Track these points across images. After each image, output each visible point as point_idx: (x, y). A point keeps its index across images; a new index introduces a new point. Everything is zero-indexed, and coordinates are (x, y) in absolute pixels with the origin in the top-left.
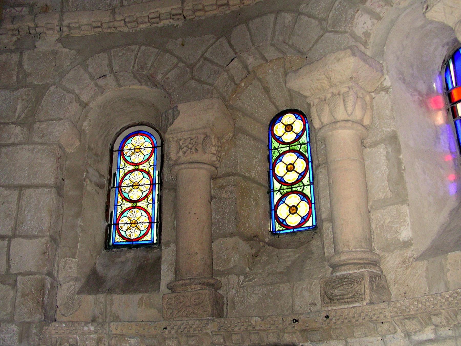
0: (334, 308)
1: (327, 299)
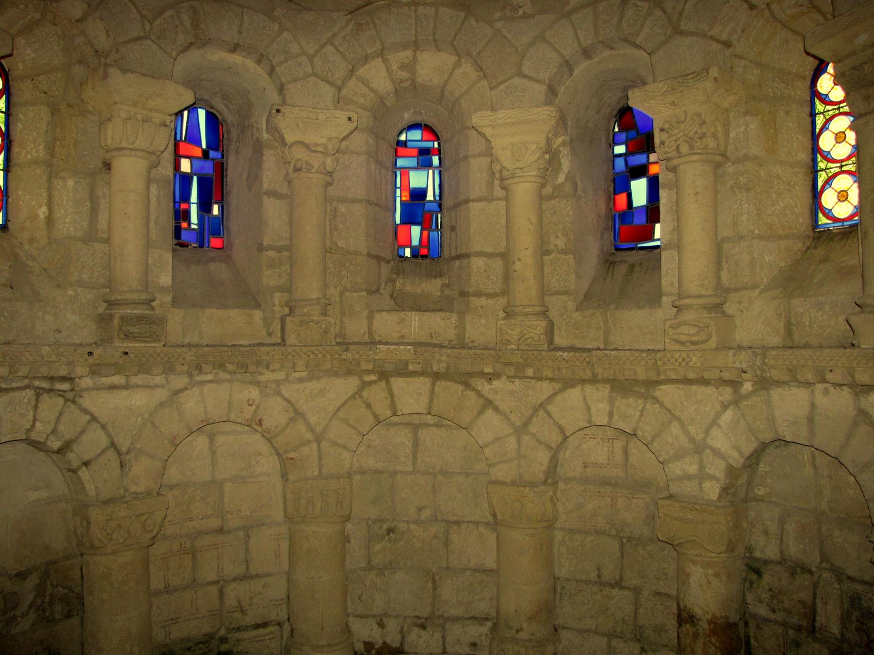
0: (130, 345)
1: (122, 336)
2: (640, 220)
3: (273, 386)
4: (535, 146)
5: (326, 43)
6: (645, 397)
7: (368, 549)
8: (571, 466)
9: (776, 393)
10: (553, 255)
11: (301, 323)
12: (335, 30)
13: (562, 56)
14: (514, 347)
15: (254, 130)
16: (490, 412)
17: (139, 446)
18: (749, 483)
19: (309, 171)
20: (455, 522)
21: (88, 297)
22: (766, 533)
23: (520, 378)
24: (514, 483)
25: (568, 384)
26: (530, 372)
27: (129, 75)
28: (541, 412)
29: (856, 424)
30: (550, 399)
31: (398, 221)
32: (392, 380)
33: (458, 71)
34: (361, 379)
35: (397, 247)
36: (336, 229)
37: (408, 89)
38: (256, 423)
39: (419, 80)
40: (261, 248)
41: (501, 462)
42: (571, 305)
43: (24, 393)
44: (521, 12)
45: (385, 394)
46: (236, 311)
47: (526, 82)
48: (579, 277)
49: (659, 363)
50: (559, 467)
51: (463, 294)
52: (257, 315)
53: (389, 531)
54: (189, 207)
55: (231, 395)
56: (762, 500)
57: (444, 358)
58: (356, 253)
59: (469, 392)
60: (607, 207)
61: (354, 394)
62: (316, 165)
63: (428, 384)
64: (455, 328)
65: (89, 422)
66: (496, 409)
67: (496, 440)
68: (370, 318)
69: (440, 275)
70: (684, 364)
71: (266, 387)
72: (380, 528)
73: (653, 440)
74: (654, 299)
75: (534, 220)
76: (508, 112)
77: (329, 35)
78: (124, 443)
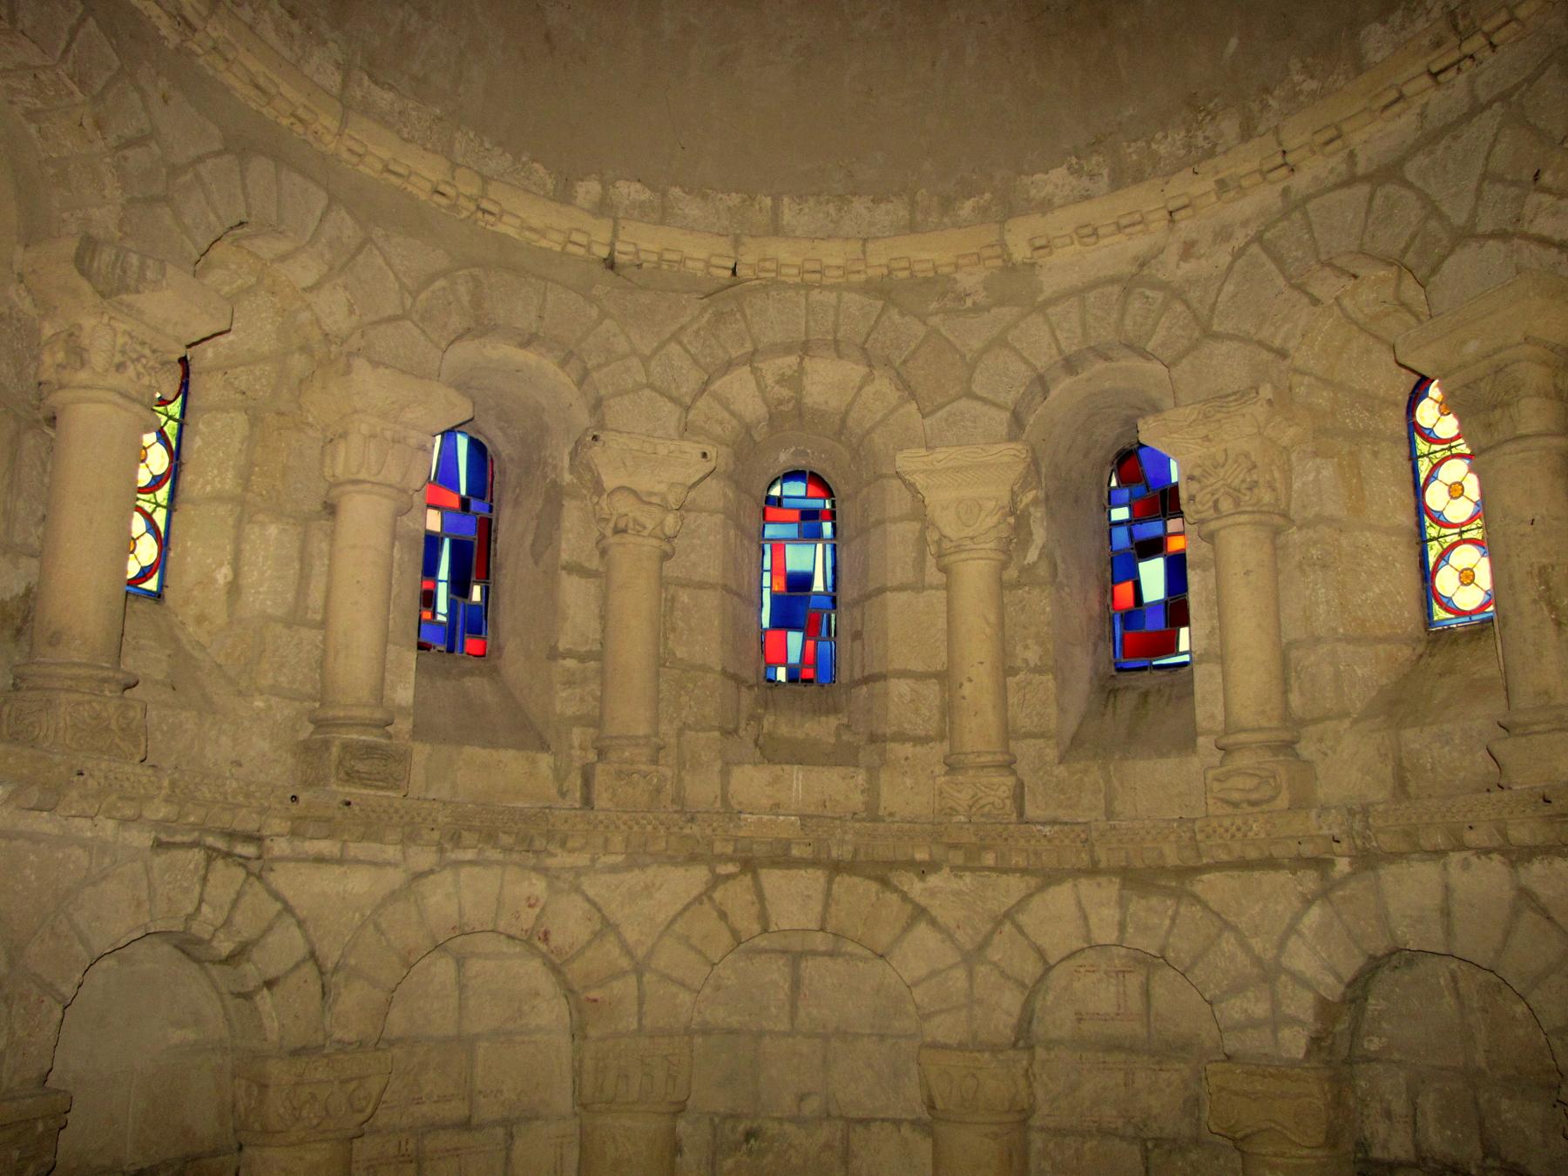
1: (342, 775)
3: (570, 876)
4: (991, 504)
5: (670, 339)
6: (1179, 895)
7: (713, 1165)
8: (1056, 1021)
9: (1388, 873)
10: (1021, 676)
11: (619, 775)
12: (685, 319)
13: (1034, 369)
14: (963, 819)
15: (548, 469)
16: (922, 929)
17: (352, 962)
18: (1355, 1032)
19: (638, 533)
20: (860, 1121)
21: (286, 712)
22: (1388, 1114)
23: (973, 870)
24: (961, 1047)
25: (1050, 878)
26: (989, 859)
27: (381, 370)
28: (1008, 927)
29: (1516, 913)
30: (1022, 904)
31: (766, 622)
32: (763, 873)
33: (869, 390)
34: (712, 871)
35: (763, 665)
36: (674, 630)
37: (791, 415)
38: (535, 940)
39: (808, 401)
40: (554, 654)
41: (941, 1011)
42: (1051, 754)
43: (190, 854)
44: (969, 302)
45: (750, 897)
46: (511, 753)
47: (978, 405)
48: (1062, 710)
49: (1199, 837)
50: (1035, 1021)
51: (873, 739)
52: (545, 761)
53: (750, 1135)
54: (436, 586)
55: (502, 887)
56: (1377, 1060)
57: (848, 837)
58: (705, 669)
59: (888, 894)
60: (1102, 603)
61: (701, 895)
62: (650, 525)
63: (822, 880)
64: (863, 792)
65: (279, 914)
66: (933, 922)
67: (933, 974)
68: (725, 774)
69: (835, 710)
70: (1239, 835)
71: (558, 878)
72: (733, 1129)
73: (1194, 964)
74: (1186, 742)
75: (992, 618)
76: (951, 450)
77: (674, 327)
78: (331, 954)
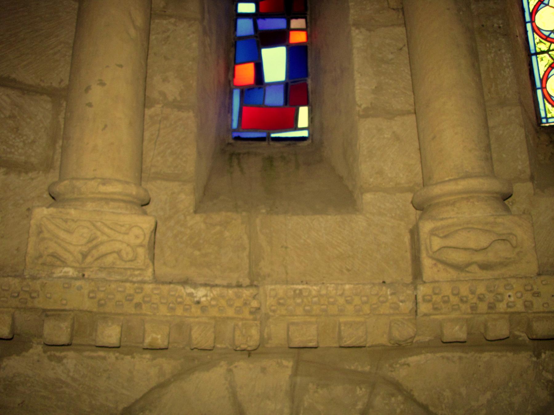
2: (275, 99)
10: (157, 108)
14: (70, 272)
42: (186, 199)
49: (424, 308)
